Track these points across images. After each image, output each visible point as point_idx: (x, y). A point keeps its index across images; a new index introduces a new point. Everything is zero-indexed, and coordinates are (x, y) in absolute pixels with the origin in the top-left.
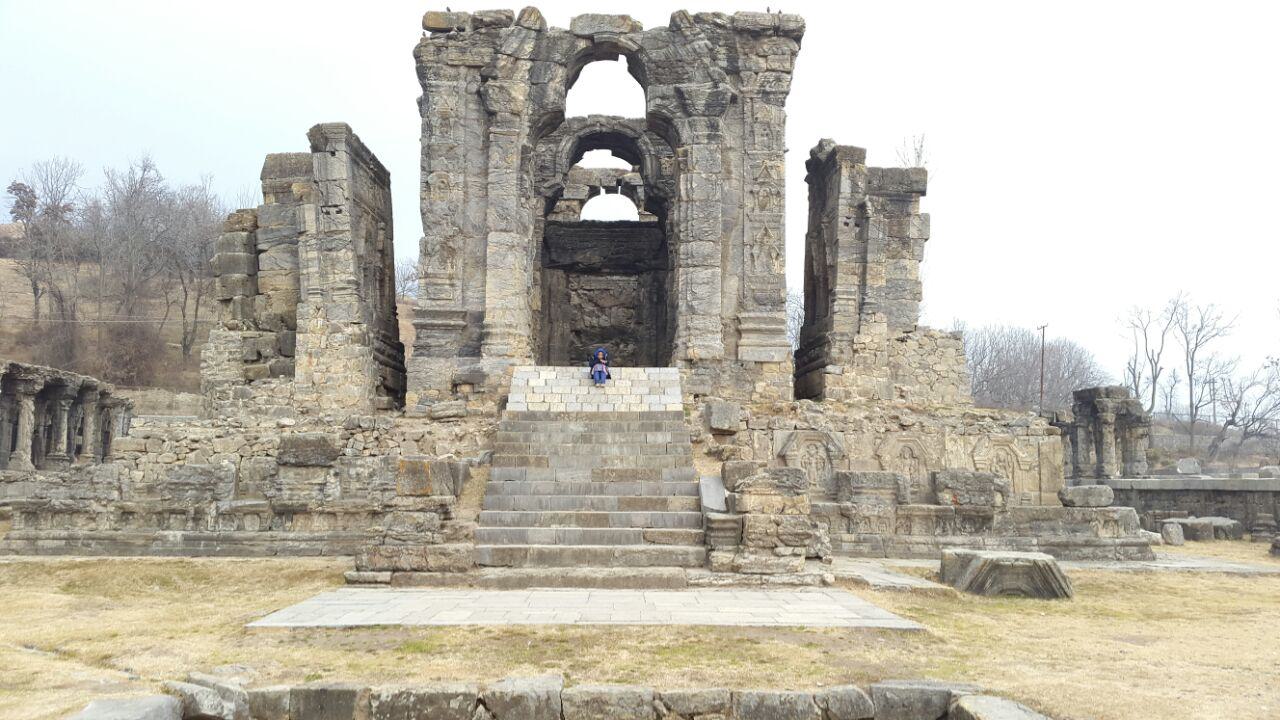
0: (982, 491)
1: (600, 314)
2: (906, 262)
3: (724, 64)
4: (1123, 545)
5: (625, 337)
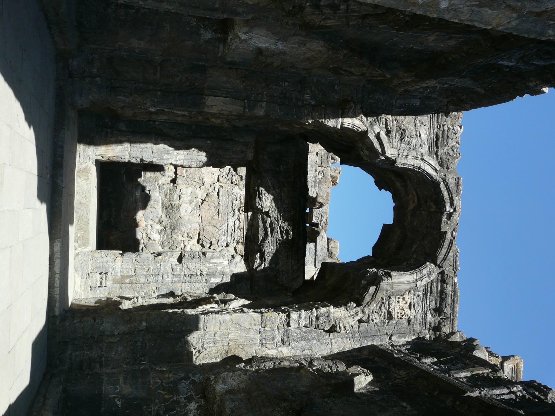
1: (194, 204)
5: (169, 231)
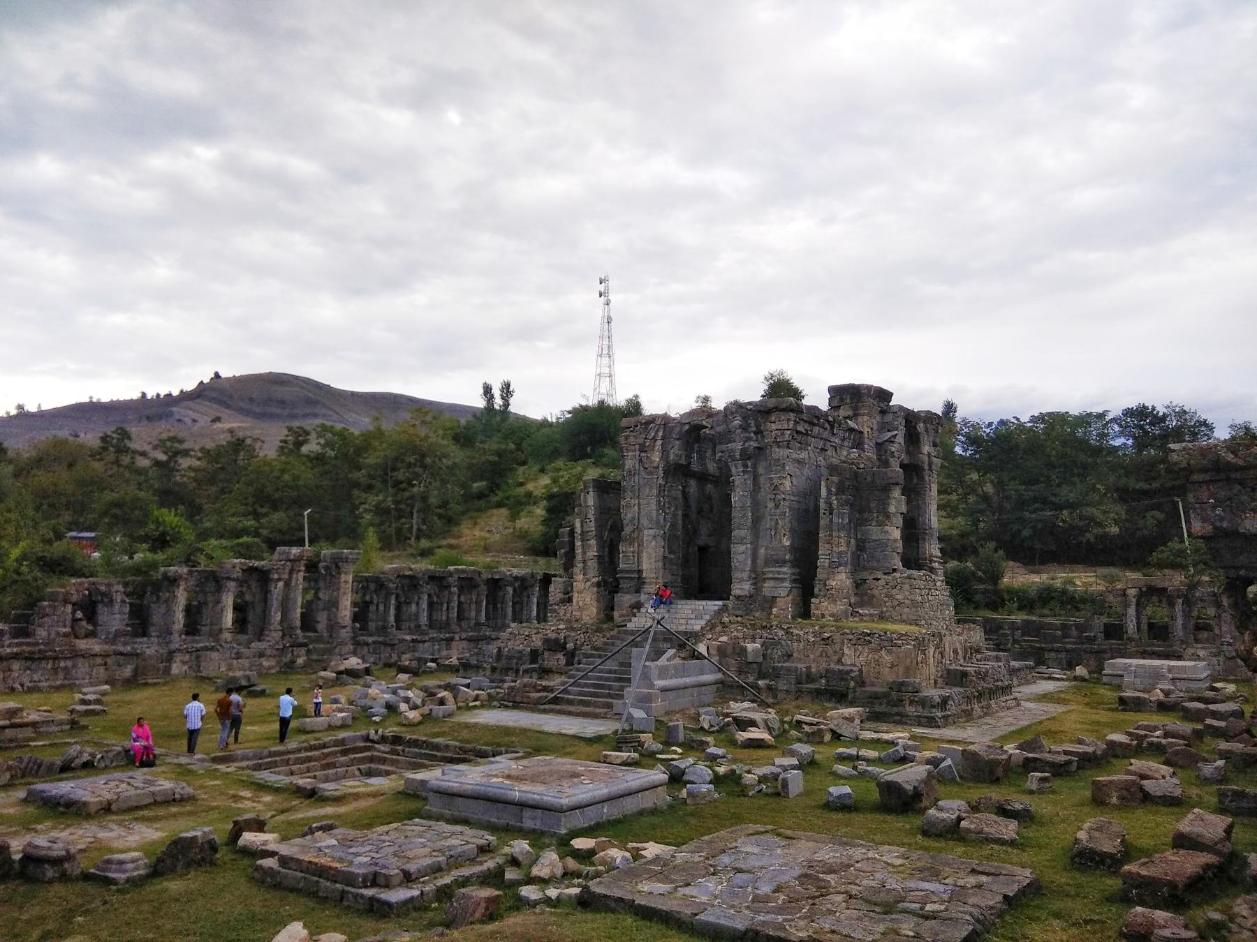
0: (842, 679)
2: (887, 528)
3: (754, 429)
4: (919, 717)
